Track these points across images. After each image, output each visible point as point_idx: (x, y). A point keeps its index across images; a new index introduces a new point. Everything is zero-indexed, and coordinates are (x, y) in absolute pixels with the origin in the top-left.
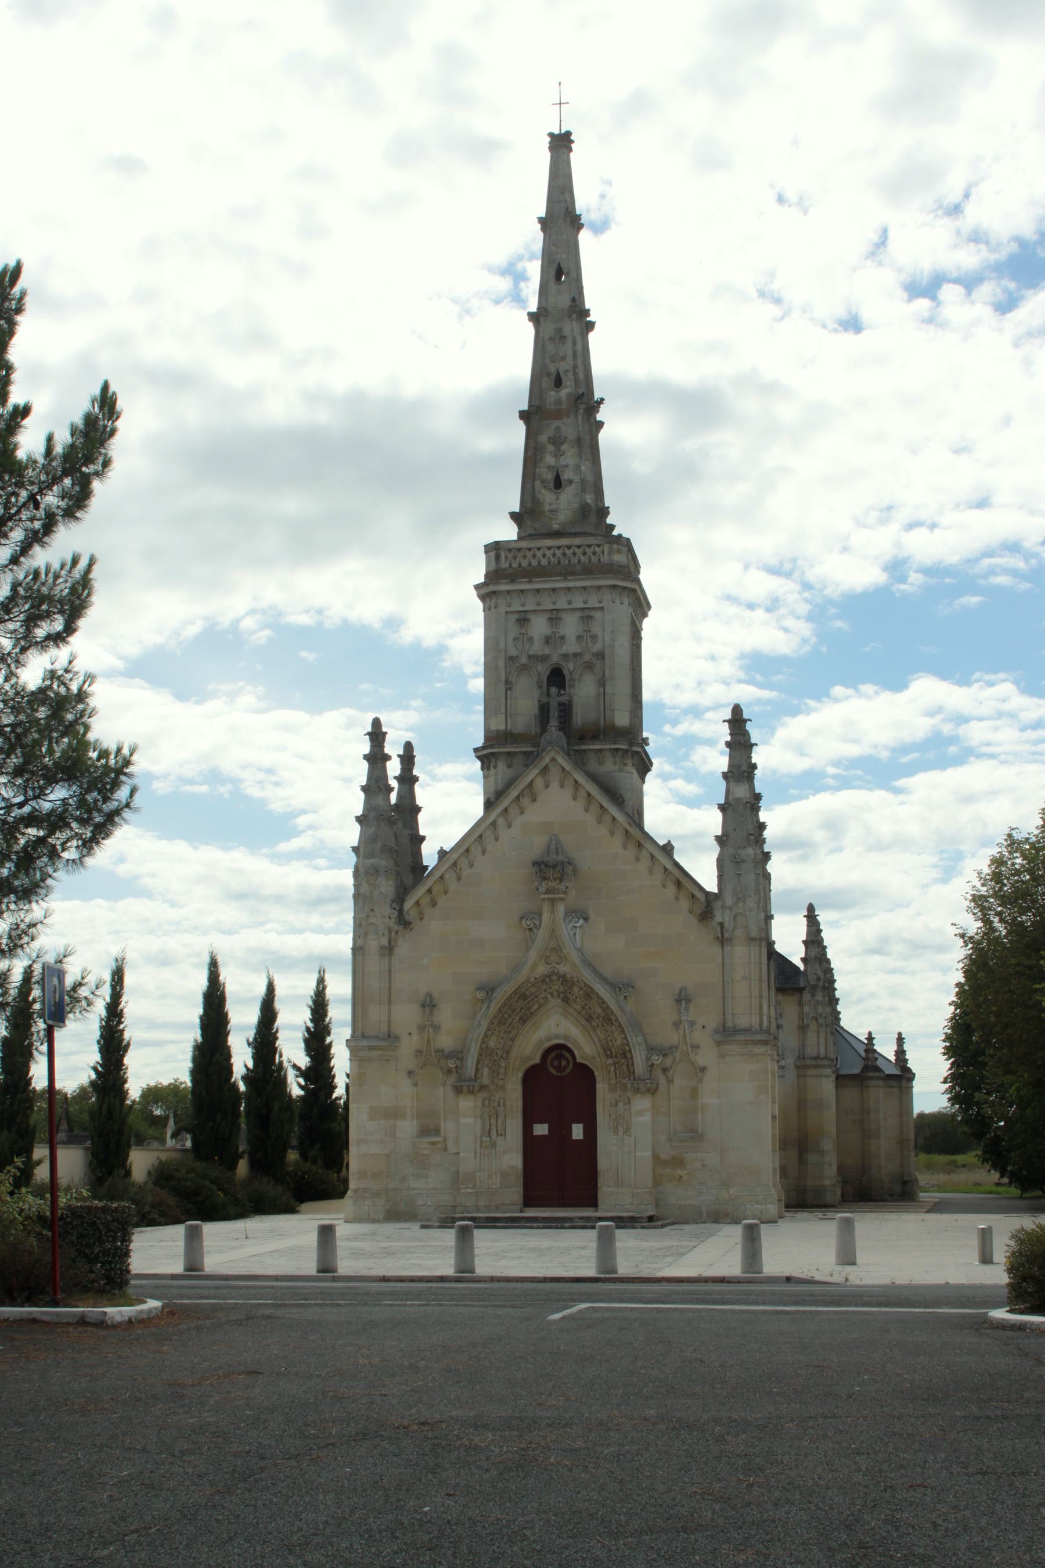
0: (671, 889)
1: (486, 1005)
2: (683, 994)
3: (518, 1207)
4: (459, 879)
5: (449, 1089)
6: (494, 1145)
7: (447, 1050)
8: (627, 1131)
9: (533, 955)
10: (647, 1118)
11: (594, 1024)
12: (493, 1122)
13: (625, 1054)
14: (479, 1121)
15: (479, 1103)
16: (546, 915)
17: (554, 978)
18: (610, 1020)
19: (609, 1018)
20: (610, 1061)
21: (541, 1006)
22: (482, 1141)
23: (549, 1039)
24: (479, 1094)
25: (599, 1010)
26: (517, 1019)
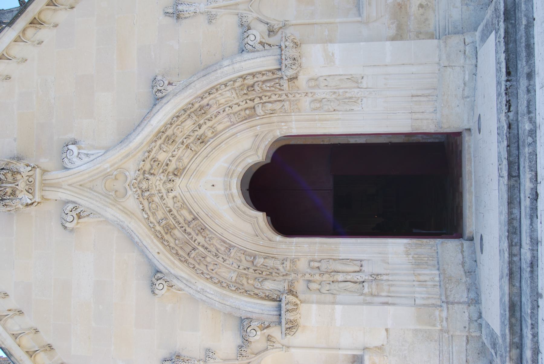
0: (44, 33)
1: (175, 282)
2: (171, 11)
3: (466, 244)
4: (20, 312)
5: (290, 340)
6: (375, 277)
7: (239, 341)
8: (355, 81)
9: (112, 213)
10: (336, 48)
11: (209, 134)
12: (340, 277)
13: (248, 85)
14: (339, 298)
15: (314, 297)
16: (63, 195)
17: (144, 185)
18: (201, 108)
19: (198, 110)
20: (259, 110)
21: (184, 205)
22: (372, 295)
23: (230, 198)
24: (301, 296)
25: (189, 122)
26: (200, 239)
